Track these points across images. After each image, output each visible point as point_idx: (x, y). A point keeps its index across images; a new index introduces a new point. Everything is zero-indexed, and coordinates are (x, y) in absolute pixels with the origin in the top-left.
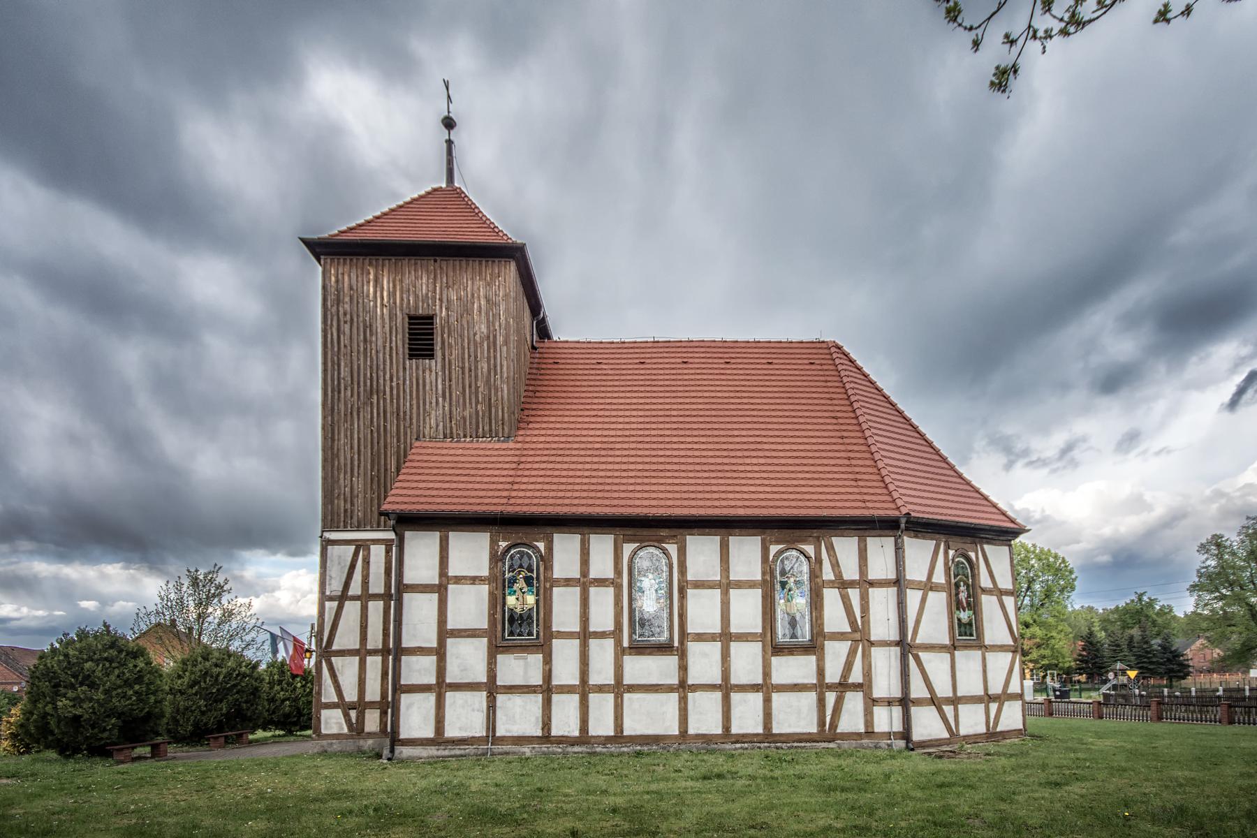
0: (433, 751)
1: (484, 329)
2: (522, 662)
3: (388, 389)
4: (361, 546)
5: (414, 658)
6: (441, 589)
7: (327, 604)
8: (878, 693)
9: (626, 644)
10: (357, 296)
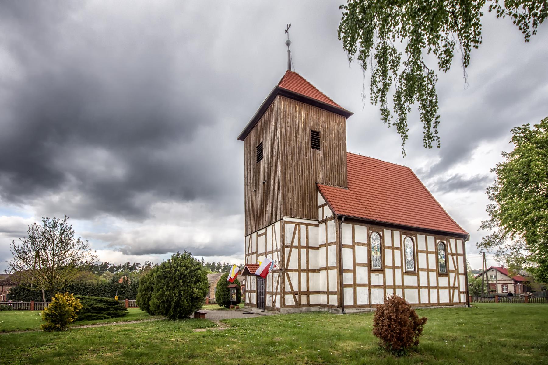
0: (354, 310)
1: (336, 142)
2: (377, 276)
3: (305, 160)
4: (297, 225)
5: (346, 274)
6: (353, 247)
7: (286, 249)
8: (461, 290)
9: (404, 271)
10: (292, 117)
